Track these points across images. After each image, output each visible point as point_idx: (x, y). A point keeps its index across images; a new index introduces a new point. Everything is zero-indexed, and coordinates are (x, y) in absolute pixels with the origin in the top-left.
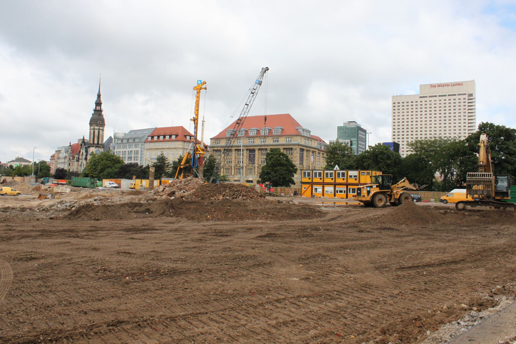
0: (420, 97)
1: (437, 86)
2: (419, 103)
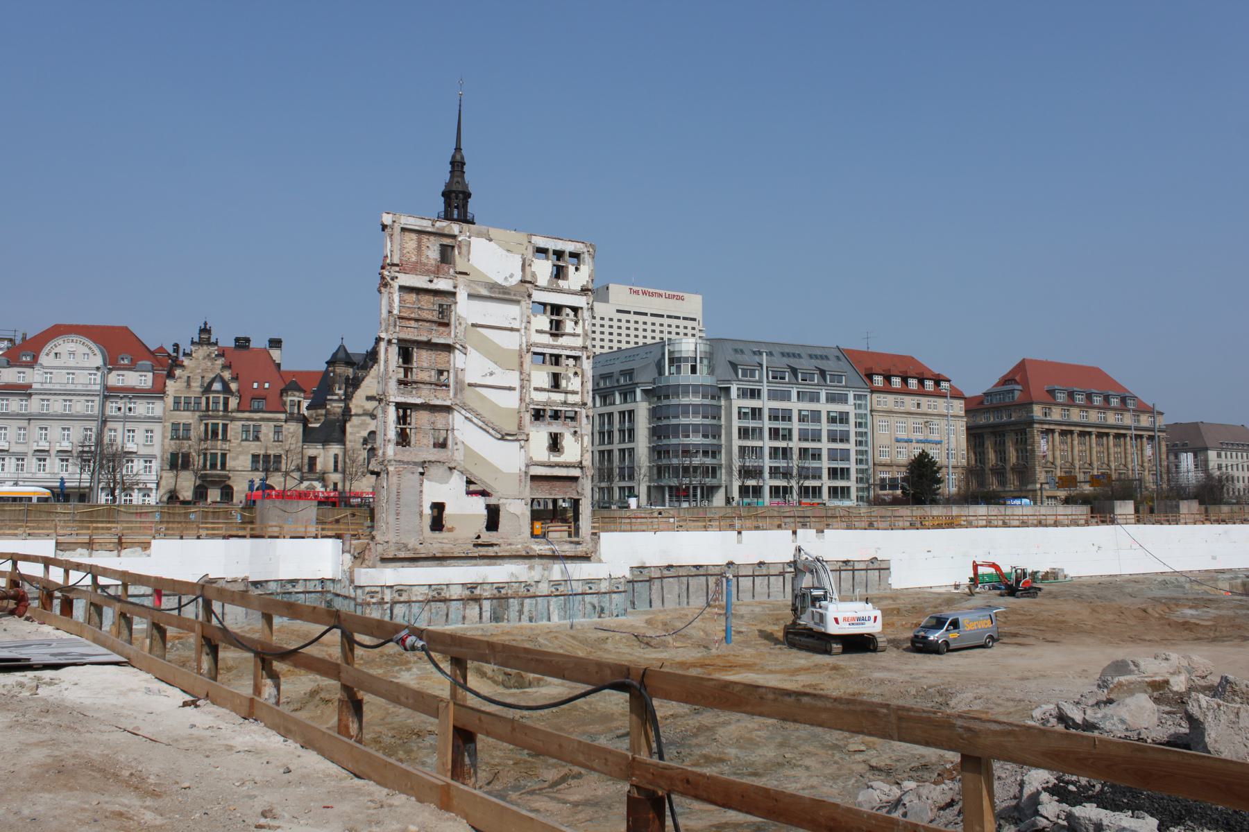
0: (618, 311)
1: (640, 292)
2: (615, 324)
